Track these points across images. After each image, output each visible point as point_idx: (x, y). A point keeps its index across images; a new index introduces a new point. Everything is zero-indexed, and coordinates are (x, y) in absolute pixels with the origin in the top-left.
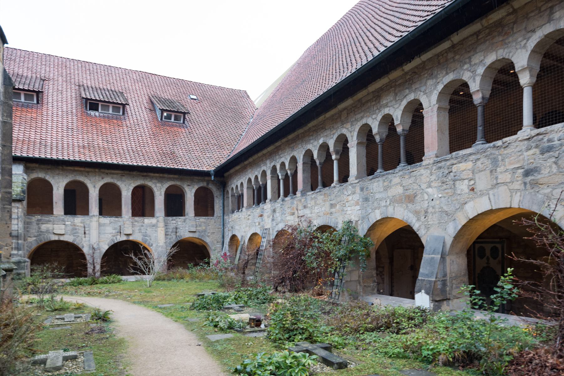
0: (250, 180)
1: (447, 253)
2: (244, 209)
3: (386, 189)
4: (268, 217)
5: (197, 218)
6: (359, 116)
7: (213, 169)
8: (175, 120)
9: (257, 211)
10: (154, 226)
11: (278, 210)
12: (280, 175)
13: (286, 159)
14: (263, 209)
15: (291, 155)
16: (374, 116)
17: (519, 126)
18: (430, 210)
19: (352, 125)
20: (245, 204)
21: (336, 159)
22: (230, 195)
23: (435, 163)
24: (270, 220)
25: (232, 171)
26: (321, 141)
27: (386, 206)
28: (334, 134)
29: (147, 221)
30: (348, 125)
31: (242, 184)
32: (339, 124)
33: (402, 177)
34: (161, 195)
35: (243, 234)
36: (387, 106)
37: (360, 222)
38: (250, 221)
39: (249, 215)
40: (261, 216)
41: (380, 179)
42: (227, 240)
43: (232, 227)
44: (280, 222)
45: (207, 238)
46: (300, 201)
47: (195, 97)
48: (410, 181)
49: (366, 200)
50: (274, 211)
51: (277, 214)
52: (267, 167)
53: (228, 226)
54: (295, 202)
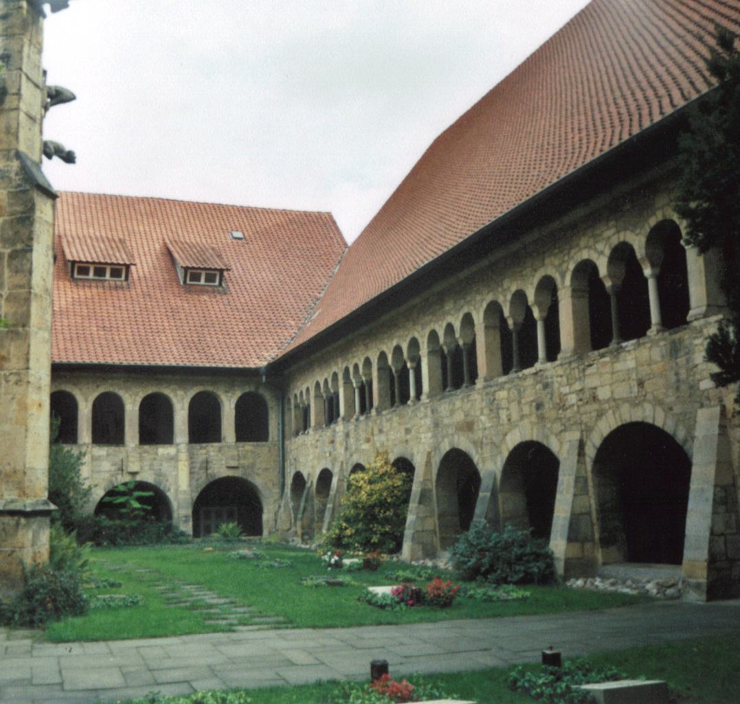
0: (318, 384)
1: (499, 490)
2: (311, 431)
3: (452, 412)
4: (341, 444)
5: (241, 444)
6: (427, 318)
7: (265, 363)
8: (206, 281)
9: (328, 433)
10: (174, 459)
11: (352, 435)
12: (354, 381)
13: (360, 360)
14: (334, 431)
15: (365, 356)
16: (440, 323)
17: (535, 359)
18: (484, 441)
19: (423, 329)
20: (313, 423)
21: (412, 368)
22: (293, 407)
23: (485, 387)
24: (343, 448)
25: (294, 368)
26: (395, 343)
27: (453, 435)
28: (406, 336)
29: (163, 450)
30: (419, 328)
31: (308, 390)
32: (411, 323)
33: (462, 399)
34: (183, 409)
35: (310, 470)
36: (448, 313)
37: (433, 453)
38: (318, 451)
39: (318, 441)
40: (333, 442)
41: (447, 400)
42: (289, 481)
43: (295, 459)
44: (355, 452)
45: (256, 477)
46: (375, 421)
47: (239, 234)
48: (469, 405)
49: (436, 425)
50: (347, 435)
51: (352, 440)
52: (338, 367)
53: (290, 457)
54: (370, 424)
